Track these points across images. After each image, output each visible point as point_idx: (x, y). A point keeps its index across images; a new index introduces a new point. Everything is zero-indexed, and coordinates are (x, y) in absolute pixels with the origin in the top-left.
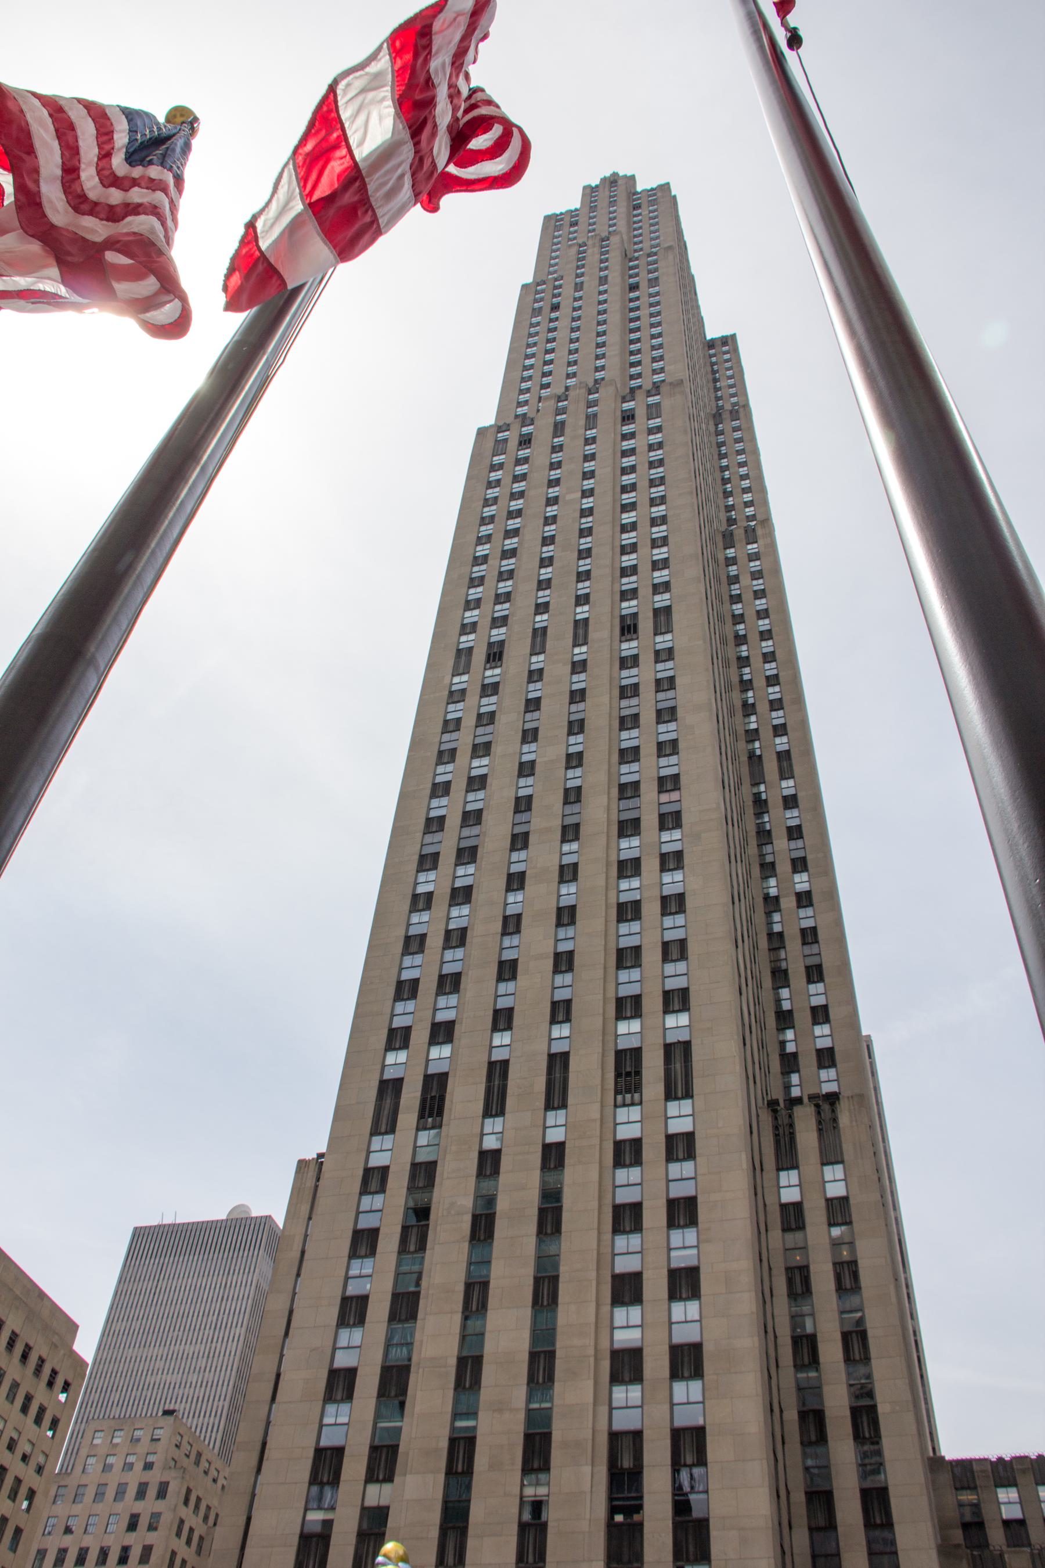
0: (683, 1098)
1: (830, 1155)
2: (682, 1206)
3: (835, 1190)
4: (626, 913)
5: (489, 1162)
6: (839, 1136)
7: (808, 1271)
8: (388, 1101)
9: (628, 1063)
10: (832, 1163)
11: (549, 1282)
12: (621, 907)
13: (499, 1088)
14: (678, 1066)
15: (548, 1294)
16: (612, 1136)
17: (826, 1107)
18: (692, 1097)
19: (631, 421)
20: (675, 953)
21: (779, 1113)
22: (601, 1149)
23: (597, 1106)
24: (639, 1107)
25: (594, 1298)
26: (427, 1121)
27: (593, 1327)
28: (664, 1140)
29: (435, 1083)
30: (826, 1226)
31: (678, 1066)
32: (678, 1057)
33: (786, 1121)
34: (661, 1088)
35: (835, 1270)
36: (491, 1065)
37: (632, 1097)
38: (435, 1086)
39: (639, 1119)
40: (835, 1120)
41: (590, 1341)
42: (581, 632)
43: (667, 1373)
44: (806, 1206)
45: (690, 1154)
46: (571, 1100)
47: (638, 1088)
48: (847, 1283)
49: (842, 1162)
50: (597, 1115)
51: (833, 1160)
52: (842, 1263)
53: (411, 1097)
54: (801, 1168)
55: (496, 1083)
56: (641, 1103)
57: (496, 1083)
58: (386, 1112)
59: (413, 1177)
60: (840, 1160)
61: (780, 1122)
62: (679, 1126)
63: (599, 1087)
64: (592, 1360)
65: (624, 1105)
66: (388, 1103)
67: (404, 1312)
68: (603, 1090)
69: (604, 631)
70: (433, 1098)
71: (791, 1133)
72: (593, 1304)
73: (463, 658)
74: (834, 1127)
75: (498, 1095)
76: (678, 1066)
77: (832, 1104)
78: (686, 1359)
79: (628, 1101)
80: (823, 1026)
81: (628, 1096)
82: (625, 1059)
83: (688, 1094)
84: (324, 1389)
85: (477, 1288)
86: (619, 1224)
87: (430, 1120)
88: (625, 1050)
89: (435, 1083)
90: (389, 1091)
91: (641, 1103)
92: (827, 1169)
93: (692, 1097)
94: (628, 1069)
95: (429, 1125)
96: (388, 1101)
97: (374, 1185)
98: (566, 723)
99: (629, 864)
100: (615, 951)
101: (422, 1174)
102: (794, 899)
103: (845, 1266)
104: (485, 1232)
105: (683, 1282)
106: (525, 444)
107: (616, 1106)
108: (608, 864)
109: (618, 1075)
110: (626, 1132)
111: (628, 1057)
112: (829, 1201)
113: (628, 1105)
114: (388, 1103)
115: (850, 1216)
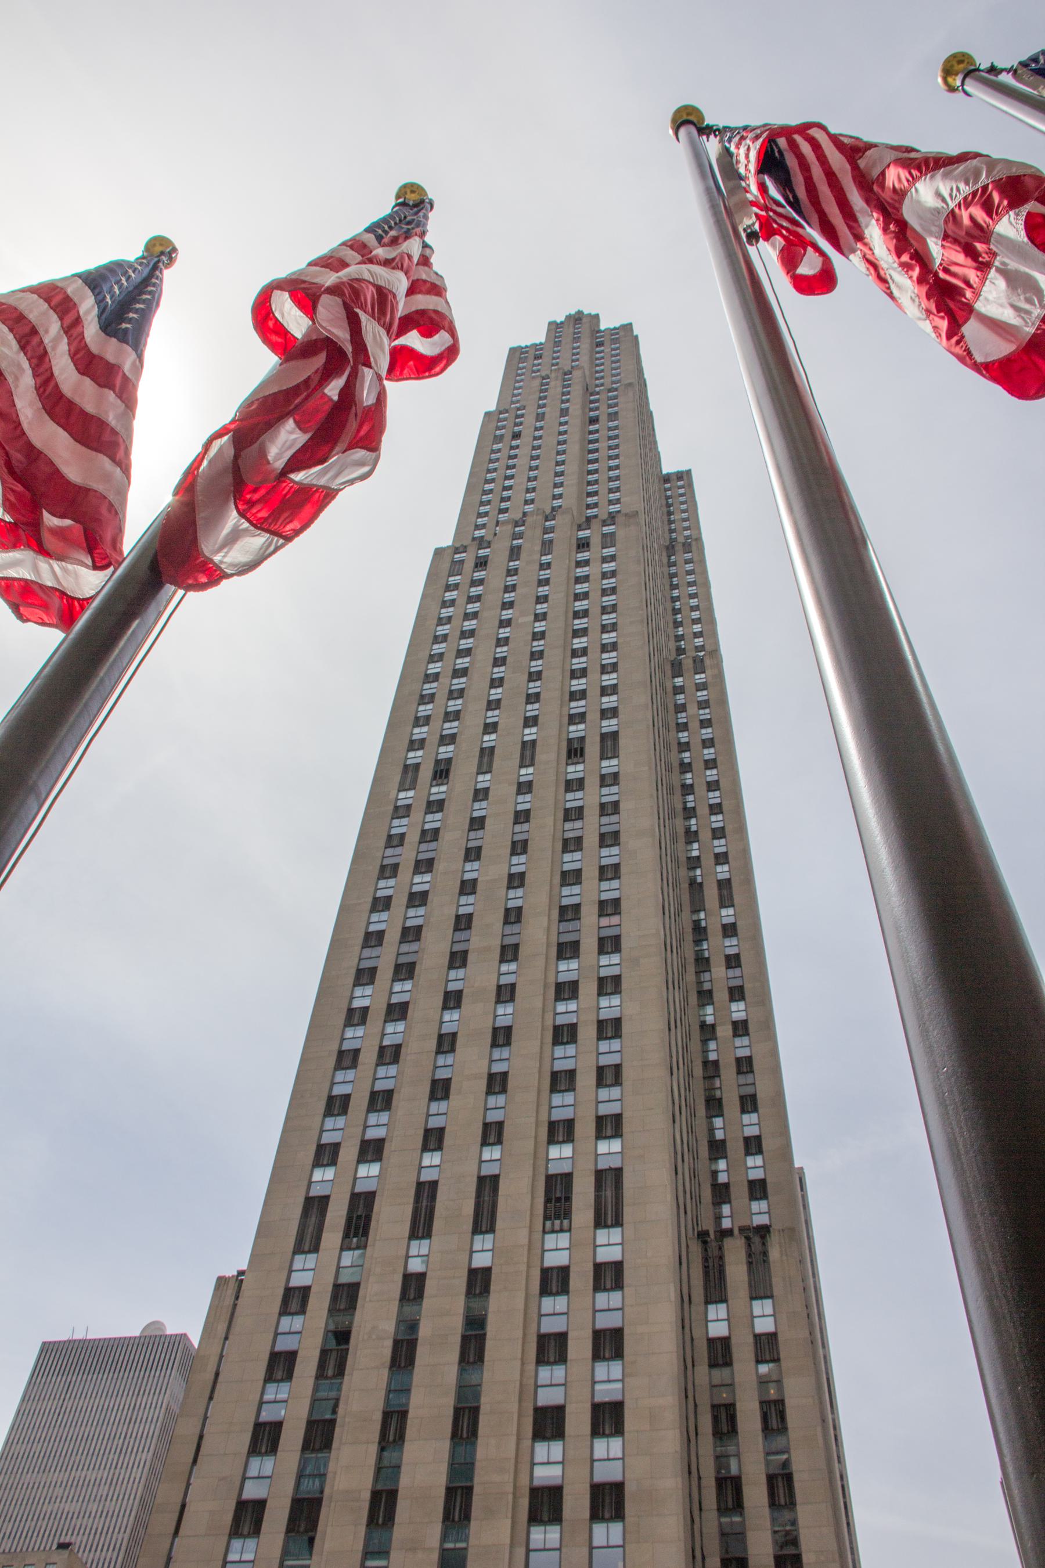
0: (612, 1226)
1: (760, 1290)
2: (608, 1337)
3: (764, 1326)
4: (562, 1036)
6: (769, 1268)
7: (735, 1410)
8: (313, 1219)
9: (558, 1187)
10: (761, 1298)
12: (557, 1030)
14: (609, 1193)
16: (539, 1264)
17: (756, 1240)
18: (622, 1225)
19: (586, 549)
20: (609, 1078)
21: (709, 1245)
23: (525, 1232)
24: (567, 1234)
25: (515, 1432)
26: (352, 1241)
27: (513, 1461)
28: (592, 1268)
29: (362, 1202)
30: (753, 1363)
31: (609, 1193)
32: (609, 1183)
33: (716, 1253)
34: (590, 1215)
35: (762, 1408)
36: (420, 1185)
37: (562, 1223)
38: (361, 1206)
39: (567, 1246)
40: (765, 1253)
41: (509, 1477)
42: (528, 753)
43: (587, 1514)
44: (733, 1341)
45: (618, 1284)
46: (499, 1224)
47: (567, 1214)
48: (774, 1423)
49: (771, 1297)
50: (525, 1241)
51: (762, 1295)
53: (337, 1214)
54: (730, 1302)
55: (424, 1204)
56: (570, 1230)
57: (424, 1204)
58: (310, 1230)
59: (335, 1297)
60: (769, 1295)
61: (710, 1254)
62: (608, 1254)
63: (528, 1213)
64: (510, 1497)
65: (553, 1231)
66: (313, 1220)
67: (318, 1440)
69: (549, 754)
70: (359, 1217)
71: (720, 1266)
72: (514, 1439)
73: (410, 774)
74: (764, 1261)
76: (609, 1193)
77: (763, 1237)
79: (557, 1227)
80: (756, 1157)
81: (557, 1222)
82: (556, 1185)
83: (618, 1222)
84: (230, 1523)
85: (395, 1418)
87: (355, 1240)
88: (556, 1175)
89: (362, 1202)
90: (315, 1210)
91: (570, 1230)
94: (558, 1195)
95: (354, 1246)
96: (313, 1219)
97: (294, 1306)
98: (509, 843)
99: (567, 987)
100: (549, 1074)
101: (344, 1297)
102: (730, 1027)
104: (406, 1359)
105: (607, 1415)
106: (481, 566)
107: (544, 1232)
108: (546, 986)
109: (548, 1200)
110: (555, 1259)
111: (559, 1181)
112: (757, 1337)
113: (557, 1232)
114: (313, 1220)
115: (778, 1354)
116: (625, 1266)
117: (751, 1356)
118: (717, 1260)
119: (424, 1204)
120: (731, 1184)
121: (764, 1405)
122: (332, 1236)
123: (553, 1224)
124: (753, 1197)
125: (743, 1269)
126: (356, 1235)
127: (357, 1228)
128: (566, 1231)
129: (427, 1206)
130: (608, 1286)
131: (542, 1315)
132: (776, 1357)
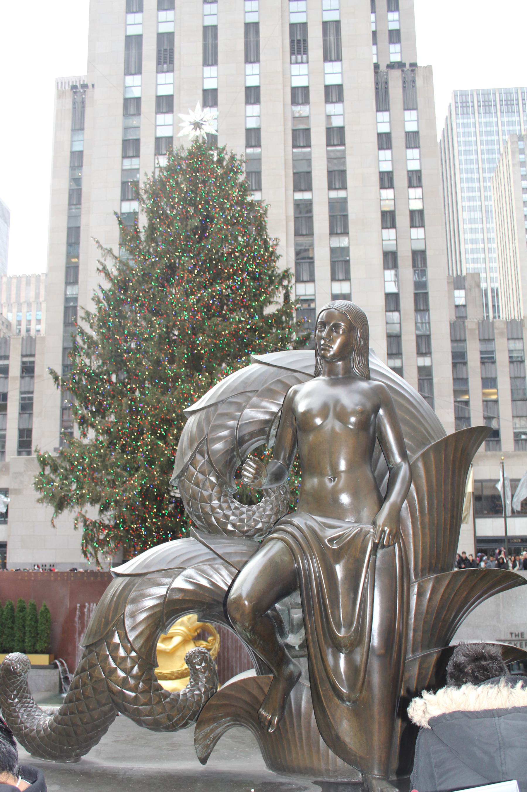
0: (335, 61)
5: (210, 97)
6: (416, 93)
7: (392, 175)
9: (298, 33)
11: (255, 176)
13: (212, 45)
14: (332, 38)
15: (255, 184)
18: (341, 60)
21: (379, 74)
22: (284, 92)
26: (163, 67)
31: (332, 38)
32: (332, 31)
34: (320, 53)
36: (205, 28)
37: (302, 58)
39: (307, 73)
40: (414, 81)
44: (393, 135)
45: (340, 99)
46: (262, 57)
49: (416, 109)
51: (411, 108)
52: (412, 171)
54: (391, 111)
60: (415, 108)
61: (379, 80)
62: (333, 80)
64: (284, 222)
65: (297, 63)
66: (134, 52)
68: (283, 52)
70: (165, 50)
71: (386, 88)
74: (413, 86)
75: (212, 51)
76: (332, 38)
78: (339, 223)
79: (299, 60)
81: (299, 57)
83: (339, 59)
86: (296, 141)
87: (165, 66)
88: (296, 24)
91: (307, 62)
92: (407, 113)
93: (341, 60)
94: (299, 38)
95: (165, 70)
97: (132, 110)
101: (164, 104)
103: (414, 173)
105: (337, 178)
107: (291, 63)
110: (299, 82)
112: (407, 133)
113: (299, 63)
115: (419, 143)
116: (344, 87)
117: (403, 144)
118: (384, 85)
119: (210, 42)
120: (378, 32)
121: (410, 173)
123: (296, 58)
124: (391, 42)
125: (400, 90)
126: (165, 63)
127: (165, 58)
129: (212, 44)
130: (334, 100)
131: (259, 116)
132: (418, 146)
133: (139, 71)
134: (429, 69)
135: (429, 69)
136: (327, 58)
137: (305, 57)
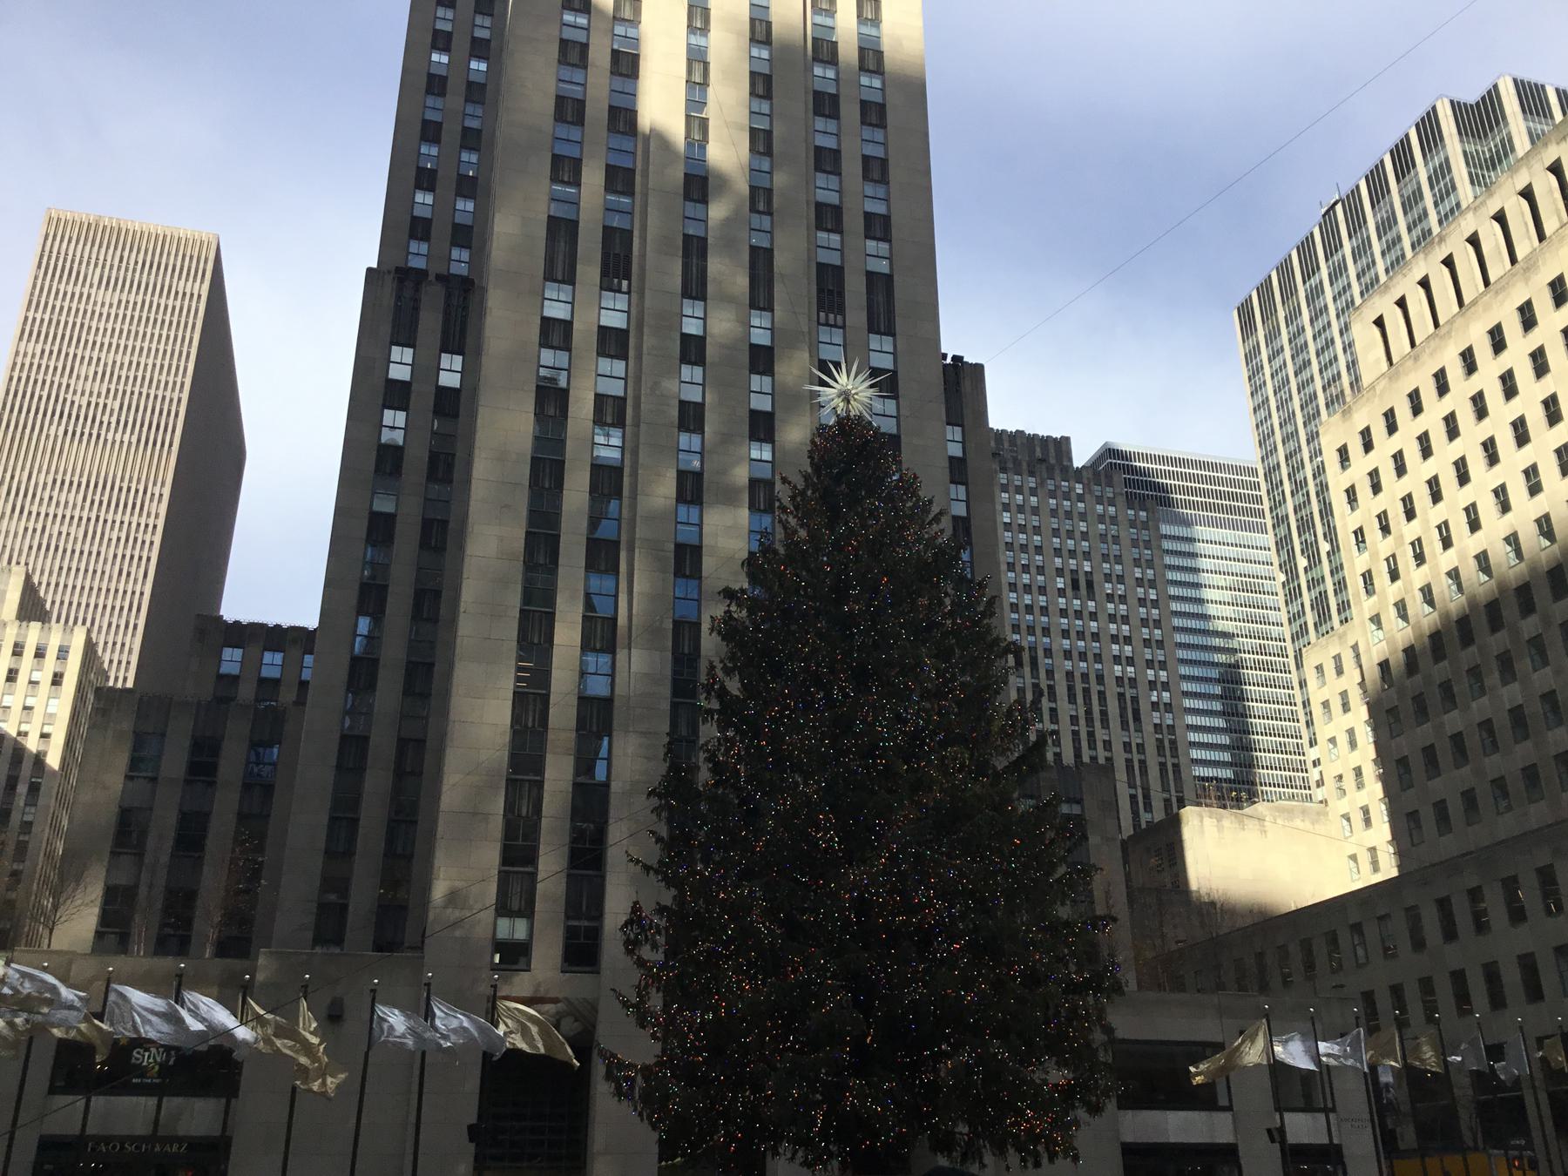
0: (885, 334)
14: (881, 298)
20: (876, 175)
40: (958, 383)
50: (806, 329)
57: (694, 261)
65: (827, 324)
66: (562, 246)
87: (616, 280)
91: (843, 327)
94: (831, 288)
96: (562, 244)
107: (819, 324)
109: (820, 291)
113: (831, 326)
122: (589, 270)
128: (840, 328)
133: (570, 279)
134: (979, 369)
135: (979, 369)
136: (873, 328)
137: (839, 317)
